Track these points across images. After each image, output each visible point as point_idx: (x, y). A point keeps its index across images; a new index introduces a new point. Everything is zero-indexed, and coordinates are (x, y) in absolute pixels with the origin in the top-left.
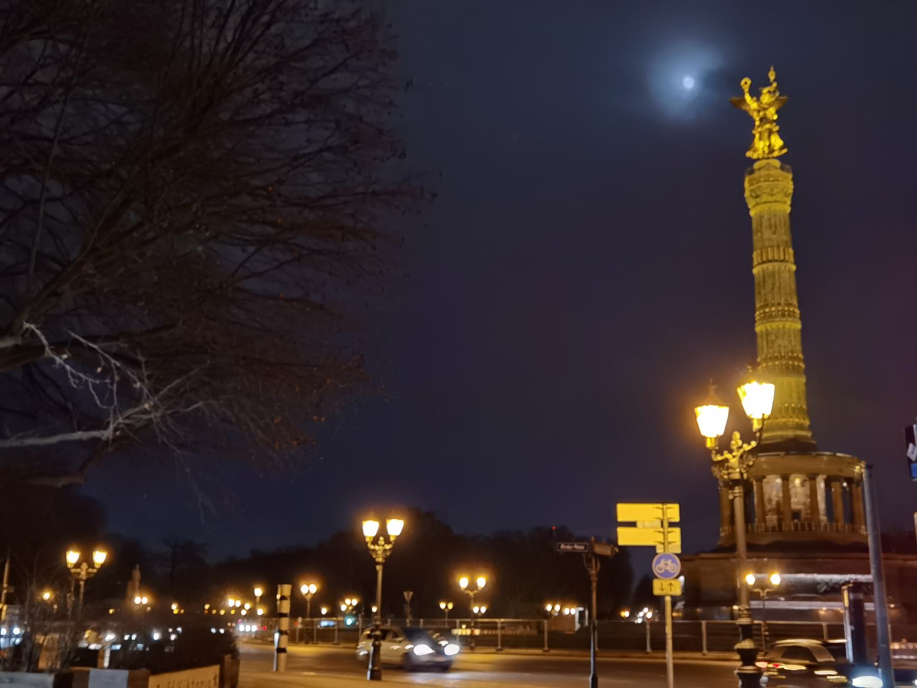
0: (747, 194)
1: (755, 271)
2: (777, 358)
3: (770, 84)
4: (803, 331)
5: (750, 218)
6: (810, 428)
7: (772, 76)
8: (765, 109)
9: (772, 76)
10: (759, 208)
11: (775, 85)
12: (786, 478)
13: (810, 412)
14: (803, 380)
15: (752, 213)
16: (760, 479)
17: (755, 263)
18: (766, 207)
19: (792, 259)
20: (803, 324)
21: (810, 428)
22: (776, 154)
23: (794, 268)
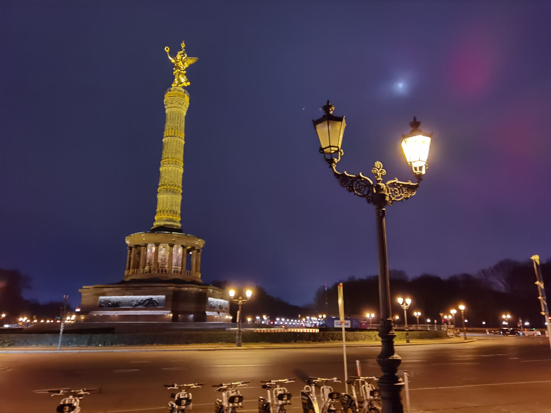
1: (163, 140)
2: (172, 185)
3: (181, 50)
4: (184, 175)
5: (166, 114)
6: (181, 222)
7: (183, 45)
8: (178, 62)
9: (183, 45)
11: (184, 50)
12: (172, 246)
13: (182, 215)
15: (167, 111)
16: (146, 246)
17: (165, 136)
18: (175, 109)
19: (183, 138)
20: (184, 170)
21: (181, 222)
22: (182, 85)
23: (184, 142)
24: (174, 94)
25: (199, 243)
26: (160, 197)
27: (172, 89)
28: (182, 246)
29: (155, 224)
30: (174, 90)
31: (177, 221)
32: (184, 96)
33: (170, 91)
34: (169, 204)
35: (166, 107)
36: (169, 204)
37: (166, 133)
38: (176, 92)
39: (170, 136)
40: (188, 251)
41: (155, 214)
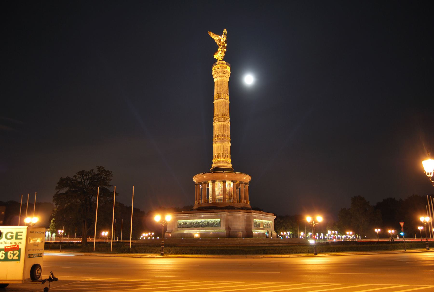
0: (213, 73)
1: (214, 102)
6: (231, 163)
10: (218, 79)
12: (224, 182)
14: (230, 144)
15: (215, 80)
17: (215, 99)
19: (228, 98)
21: (231, 163)
23: (229, 102)
24: (218, 67)
25: (247, 178)
26: (214, 145)
27: (217, 63)
28: (232, 181)
29: (213, 166)
30: (218, 64)
31: (228, 163)
32: (226, 67)
33: (216, 65)
34: (221, 150)
35: (214, 77)
36: (221, 150)
37: (215, 97)
38: (220, 65)
39: (218, 99)
40: (239, 184)
41: (212, 158)
